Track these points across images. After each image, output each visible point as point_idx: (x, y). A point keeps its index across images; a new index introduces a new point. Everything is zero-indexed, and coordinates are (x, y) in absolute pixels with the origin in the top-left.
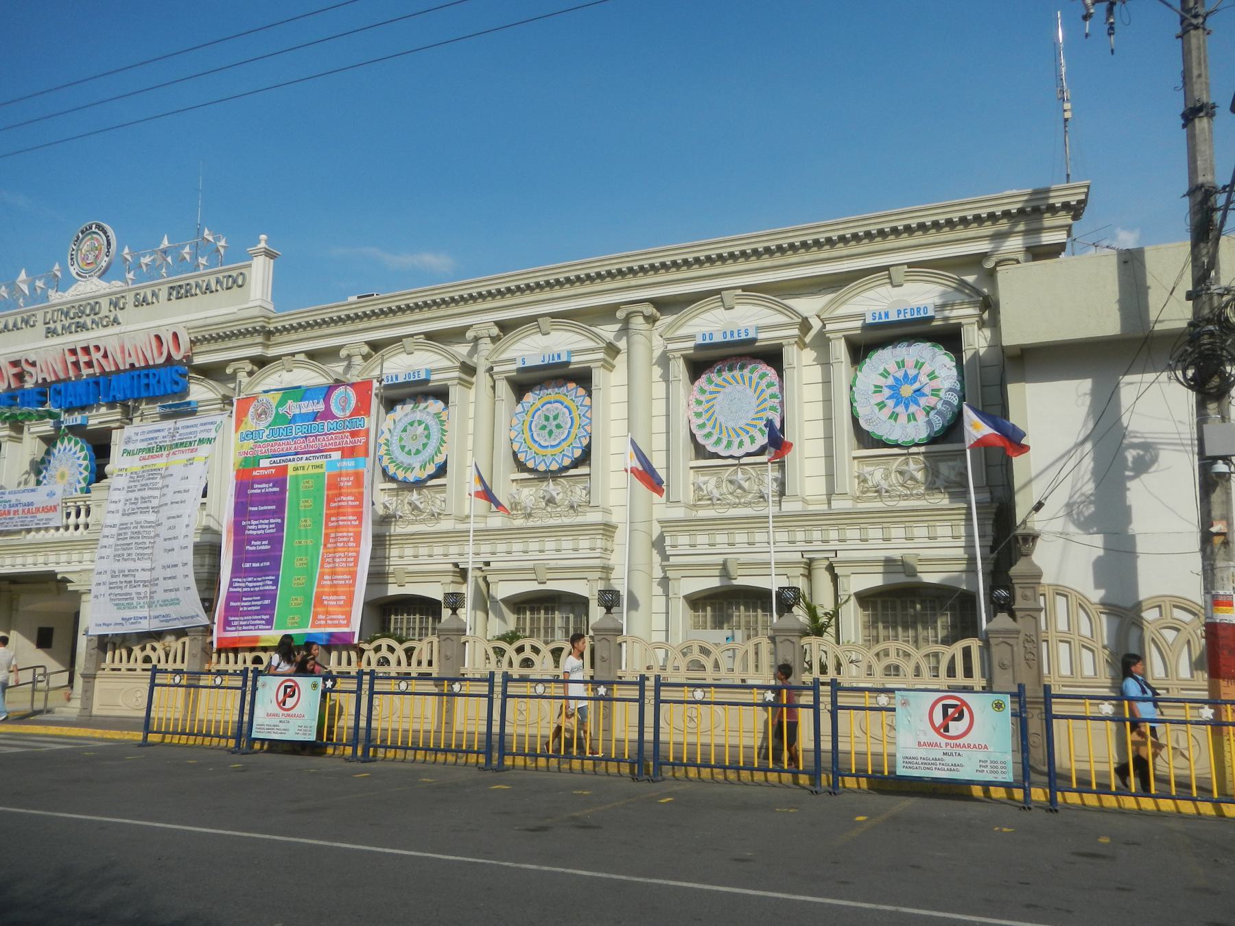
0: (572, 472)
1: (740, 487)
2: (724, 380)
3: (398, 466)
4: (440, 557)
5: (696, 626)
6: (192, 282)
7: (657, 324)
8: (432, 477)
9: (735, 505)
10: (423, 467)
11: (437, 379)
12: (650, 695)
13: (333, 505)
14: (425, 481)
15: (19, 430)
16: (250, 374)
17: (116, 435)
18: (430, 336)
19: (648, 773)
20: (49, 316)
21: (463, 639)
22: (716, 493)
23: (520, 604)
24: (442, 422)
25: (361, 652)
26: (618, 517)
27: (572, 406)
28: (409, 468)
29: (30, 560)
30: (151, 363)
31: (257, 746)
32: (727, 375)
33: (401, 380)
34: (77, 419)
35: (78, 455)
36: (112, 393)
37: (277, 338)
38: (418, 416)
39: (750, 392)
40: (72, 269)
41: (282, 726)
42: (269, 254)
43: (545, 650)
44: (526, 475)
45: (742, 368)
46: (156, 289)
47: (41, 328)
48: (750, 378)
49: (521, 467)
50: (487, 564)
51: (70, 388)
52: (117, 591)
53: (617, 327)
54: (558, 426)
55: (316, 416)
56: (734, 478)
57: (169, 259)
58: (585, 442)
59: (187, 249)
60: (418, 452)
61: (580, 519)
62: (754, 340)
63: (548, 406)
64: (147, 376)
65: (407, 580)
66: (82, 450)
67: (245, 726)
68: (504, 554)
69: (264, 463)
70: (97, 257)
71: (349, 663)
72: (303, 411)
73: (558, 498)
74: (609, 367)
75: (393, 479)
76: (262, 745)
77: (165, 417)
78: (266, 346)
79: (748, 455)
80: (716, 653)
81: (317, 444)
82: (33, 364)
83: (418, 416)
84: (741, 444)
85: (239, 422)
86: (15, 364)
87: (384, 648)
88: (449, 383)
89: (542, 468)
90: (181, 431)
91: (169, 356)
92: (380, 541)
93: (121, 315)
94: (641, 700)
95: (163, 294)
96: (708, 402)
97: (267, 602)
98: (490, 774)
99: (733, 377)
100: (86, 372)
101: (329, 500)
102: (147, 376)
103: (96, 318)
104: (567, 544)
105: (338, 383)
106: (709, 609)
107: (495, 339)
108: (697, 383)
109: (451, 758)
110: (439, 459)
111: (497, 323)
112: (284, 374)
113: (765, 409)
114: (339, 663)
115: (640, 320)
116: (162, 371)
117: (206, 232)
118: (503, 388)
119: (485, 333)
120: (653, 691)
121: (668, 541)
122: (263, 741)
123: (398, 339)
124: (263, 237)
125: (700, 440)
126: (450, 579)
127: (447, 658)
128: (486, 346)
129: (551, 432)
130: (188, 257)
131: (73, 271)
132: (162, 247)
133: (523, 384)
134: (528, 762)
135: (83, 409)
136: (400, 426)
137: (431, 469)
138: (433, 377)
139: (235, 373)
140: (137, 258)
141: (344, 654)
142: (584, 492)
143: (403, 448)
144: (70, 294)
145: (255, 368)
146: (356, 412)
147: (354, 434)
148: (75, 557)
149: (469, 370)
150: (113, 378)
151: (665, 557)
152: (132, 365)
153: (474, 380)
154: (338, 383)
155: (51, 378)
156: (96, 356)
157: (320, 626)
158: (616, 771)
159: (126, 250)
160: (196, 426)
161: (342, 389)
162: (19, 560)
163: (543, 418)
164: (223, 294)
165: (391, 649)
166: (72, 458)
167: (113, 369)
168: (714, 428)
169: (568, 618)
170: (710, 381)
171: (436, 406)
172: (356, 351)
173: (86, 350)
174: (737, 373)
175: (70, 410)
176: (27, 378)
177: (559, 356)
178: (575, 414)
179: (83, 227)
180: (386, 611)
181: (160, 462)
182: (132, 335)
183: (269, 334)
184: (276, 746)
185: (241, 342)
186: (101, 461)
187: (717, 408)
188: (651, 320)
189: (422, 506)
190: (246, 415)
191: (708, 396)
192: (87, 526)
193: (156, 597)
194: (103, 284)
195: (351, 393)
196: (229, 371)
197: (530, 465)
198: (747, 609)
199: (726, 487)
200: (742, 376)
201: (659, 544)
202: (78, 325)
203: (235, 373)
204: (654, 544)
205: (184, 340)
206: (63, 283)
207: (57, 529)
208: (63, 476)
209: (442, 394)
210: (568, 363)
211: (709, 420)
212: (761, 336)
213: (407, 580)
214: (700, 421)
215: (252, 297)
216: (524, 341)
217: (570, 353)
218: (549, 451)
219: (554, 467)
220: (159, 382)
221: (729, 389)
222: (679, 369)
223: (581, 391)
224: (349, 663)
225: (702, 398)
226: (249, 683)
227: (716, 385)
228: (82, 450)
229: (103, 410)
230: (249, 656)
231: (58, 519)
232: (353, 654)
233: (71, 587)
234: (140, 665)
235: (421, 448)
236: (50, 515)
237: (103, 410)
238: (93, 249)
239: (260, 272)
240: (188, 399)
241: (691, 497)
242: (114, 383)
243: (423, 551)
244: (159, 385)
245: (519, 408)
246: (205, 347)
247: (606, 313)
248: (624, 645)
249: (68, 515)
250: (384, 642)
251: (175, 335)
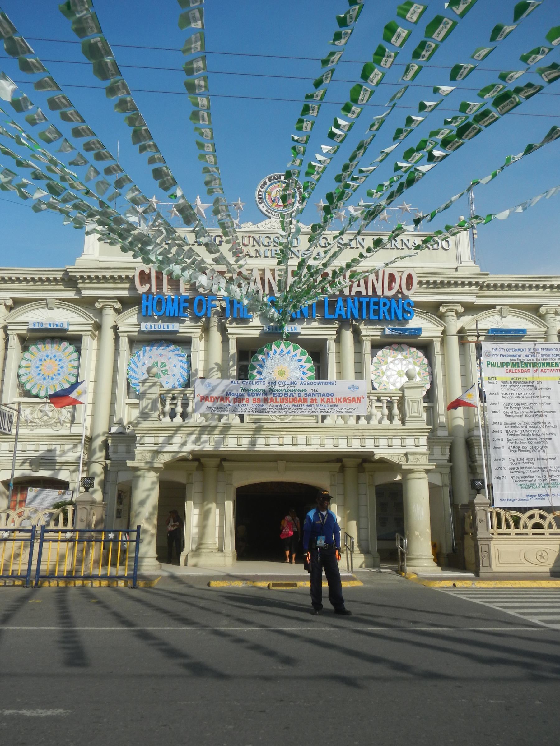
30: (379, 293)
35: (298, 357)
37: (486, 292)
40: (261, 206)
66: (302, 354)
148: (396, 441)
152: (359, 294)
162: (329, 441)
179: (271, 176)
196: (442, 309)
205: (415, 281)
220: (389, 311)
228: (302, 354)
229: (315, 324)
234: (530, 531)
236: (354, 405)
251: (410, 277)
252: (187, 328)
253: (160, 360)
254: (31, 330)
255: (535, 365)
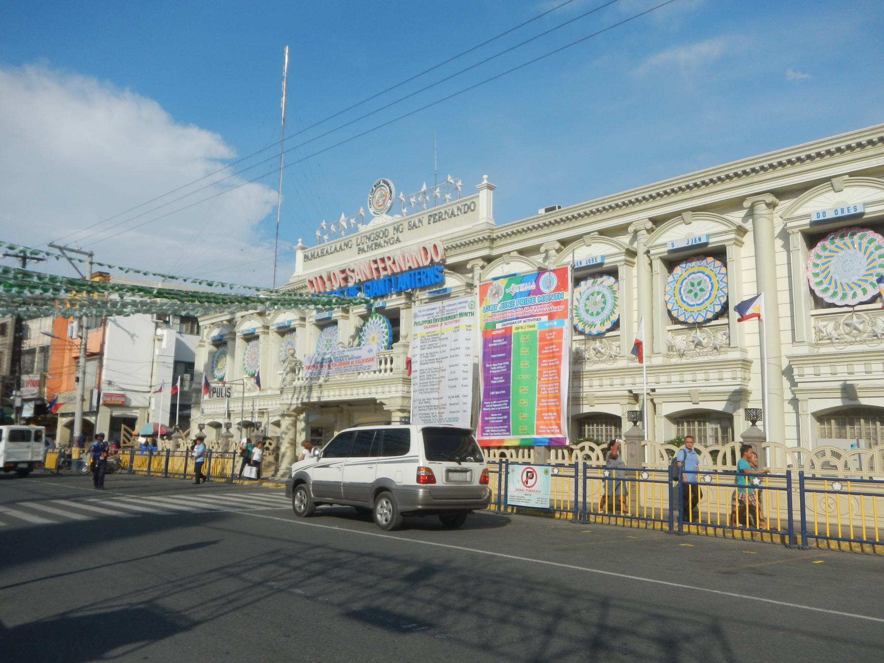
0: (714, 323)
1: (856, 329)
2: (837, 246)
3: (585, 324)
4: (620, 386)
5: (823, 436)
6: (443, 211)
7: (777, 208)
8: (609, 330)
9: (851, 343)
10: (603, 323)
11: (609, 262)
12: (796, 486)
13: (543, 352)
14: (604, 333)
15: (346, 311)
16: (483, 267)
17: (403, 313)
18: (602, 232)
19: (796, 543)
20: (359, 241)
21: (643, 443)
22: (835, 334)
23: (677, 419)
24: (614, 292)
25: (571, 451)
26: (753, 354)
27: (712, 275)
28: (592, 325)
29: (361, 391)
30: (421, 265)
31: (509, 510)
32: (838, 242)
33: (584, 264)
34: (379, 303)
36: (399, 286)
38: (597, 288)
39: (860, 254)
41: (527, 498)
42: (490, 187)
43: (706, 452)
44: (679, 326)
45: (853, 234)
46: (420, 217)
47: (355, 249)
48: (860, 244)
49: (675, 321)
50: (653, 390)
51: (375, 285)
52: (423, 412)
53: (742, 213)
54: (702, 290)
55: (530, 293)
56: (849, 322)
57: (427, 198)
58: (724, 300)
59: (438, 190)
60: (598, 313)
61: (722, 357)
62: (863, 214)
63: (693, 275)
64: (419, 273)
65: (596, 402)
67: (503, 498)
68: (665, 383)
69: (499, 326)
70: (384, 201)
71: (563, 458)
72: (522, 290)
73: (704, 342)
74: (739, 243)
75: (581, 333)
76: (513, 509)
77: (432, 300)
78: (491, 248)
79: (861, 303)
80: (845, 457)
81: (531, 311)
82: (353, 271)
83: (597, 288)
84: (855, 295)
85: (482, 300)
86: (343, 272)
87: (587, 448)
88: (618, 264)
89: (691, 321)
90: (447, 308)
91: (432, 260)
92: (576, 376)
93: (400, 236)
94: (789, 489)
95: (425, 221)
96: (823, 264)
97: (506, 417)
98: (674, 537)
99: (845, 244)
100: (383, 273)
101: (541, 348)
102: (419, 273)
103: (386, 239)
104: (714, 375)
105: (542, 271)
106: (833, 421)
107: (650, 231)
108: (813, 251)
109: (642, 525)
110: (614, 318)
111: (651, 219)
112: (504, 265)
113: (874, 267)
114: (557, 458)
115: (764, 206)
116: (428, 269)
117: (449, 177)
118: (659, 266)
119: (642, 227)
120: (797, 484)
121: (796, 372)
122: (513, 506)
123: (579, 237)
124: (485, 176)
125: (818, 294)
126: (626, 401)
127: (632, 455)
128: (643, 236)
129: (696, 295)
130: (439, 195)
131: (371, 211)
132: (423, 190)
133: (671, 262)
134: (700, 530)
135: (382, 297)
136: (584, 297)
137: (608, 325)
138: (606, 261)
139: (472, 268)
140: (408, 198)
141: (560, 451)
142: (724, 337)
143: (587, 311)
144: (371, 226)
145: (485, 264)
146: (558, 289)
147: (557, 304)
148: (387, 389)
149: (632, 253)
150: (399, 276)
151: (794, 384)
152: (410, 268)
153: (635, 260)
154: (542, 271)
155: (363, 279)
156: (389, 263)
157: (541, 434)
158: (769, 540)
159: (401, 195)
160: (455, 304)
161: (547, 274)
162: (355, 392)
163: (689, 285)
164: (462, 217)
165: (592, 449)
166: (378, 327)
167: (399, 270)
168: (830, 284)
169: (716, 429)
170: (824, 248)
171: (609, 280)
172: (551, 247)
173: (383, 260)
174: (847, 239)
175: (375, 298)
176: (350, 279)
177: (700, 239)
178: (714, 280)
179: (375, 183)
180: (581, 422)
181: (437, 330)
182: (409, 249)
183: (493, 240)
184: (522, 510)
185: (476, 246)
186: (395, 329)
187: (832, 269)
188: (771, 206)
189: (603, 351)
190: (486, 295)
191: (824, 260)
192: (391, 370)
193: (444, 416)
194: (389, 217)
195: (553, 275)
196: (469, 266)
197: (682, 319)
198: (867, 421)
199: (842, 329)
200: (853, 244)
201: (788, 372)
202: (376, 245)
203: (472, 268)
204: (783, 373)
206: (365, 220)
207: (375, 372)
208: (373, 339)
209: (613, 272)
210: (706, 244)
211: (825, 278)
212: (868, 210)
213: (596, 402)
214: (818, 280)
215: (481, 217)
216: (671, 230)
217: (708, 236)
218: (696, 308)
219: (700, 319)
221: (841, 253)
222: (798, 241)
223: (718, 263)
224: (563, 458)
225: (819, 262)
226: (504, 470)
227: (830, 251)
229: (394, 296)
230: (498, 452)
231: (375, 366)
232: (566, 452)
233: (385, 408)
235: (600, 310)
236: (370, 363)
237: (394, 296)
238: (382, 196)
239: (484, 200)
240: (445, 287)
241: (813, 338)
242: (400, 279)
243: (606, 382)
244: (426, 279)
245: (671, 279)
246: (453, 252)
247: (736, 204)
248: (768, 449)
249: (381, 363)
250: (587, 444)
251: (435, 247)
252: (337, 314)
253: (330, 338)
254: (279, 328)
255: (442, 319)
